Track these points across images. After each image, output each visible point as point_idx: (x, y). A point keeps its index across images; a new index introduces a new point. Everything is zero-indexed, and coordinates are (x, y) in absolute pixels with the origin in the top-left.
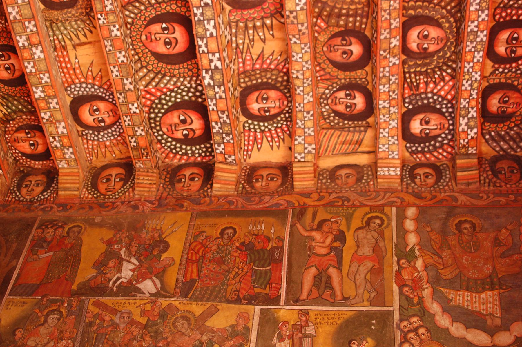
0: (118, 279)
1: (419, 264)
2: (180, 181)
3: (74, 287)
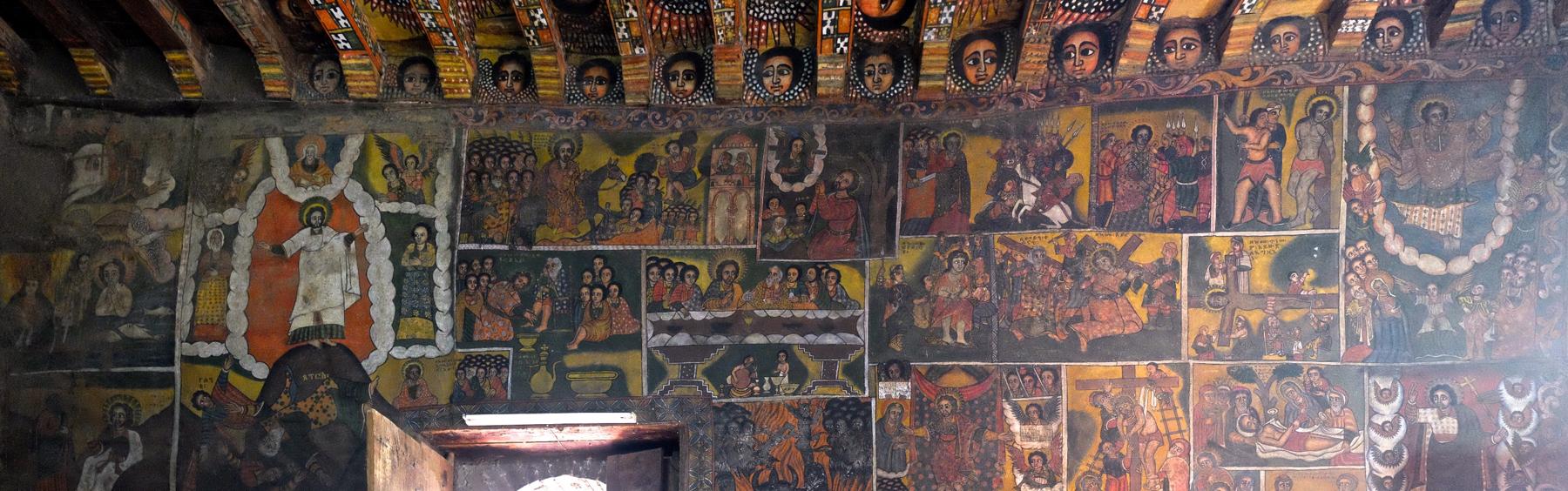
0: (1021, 206)
1: (1373, 170)
2: (1068, 57)
3: (972, 220)
